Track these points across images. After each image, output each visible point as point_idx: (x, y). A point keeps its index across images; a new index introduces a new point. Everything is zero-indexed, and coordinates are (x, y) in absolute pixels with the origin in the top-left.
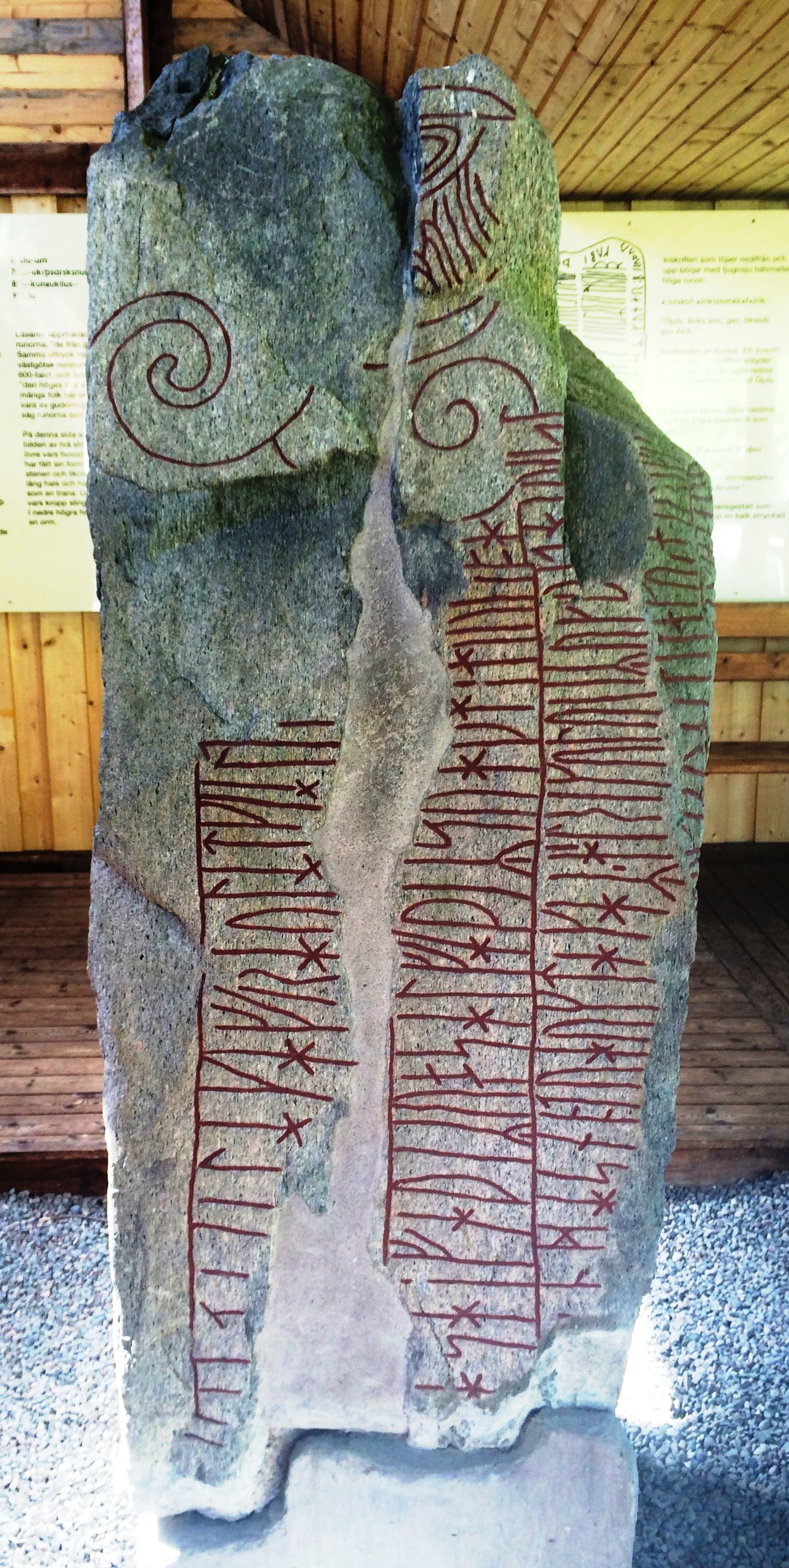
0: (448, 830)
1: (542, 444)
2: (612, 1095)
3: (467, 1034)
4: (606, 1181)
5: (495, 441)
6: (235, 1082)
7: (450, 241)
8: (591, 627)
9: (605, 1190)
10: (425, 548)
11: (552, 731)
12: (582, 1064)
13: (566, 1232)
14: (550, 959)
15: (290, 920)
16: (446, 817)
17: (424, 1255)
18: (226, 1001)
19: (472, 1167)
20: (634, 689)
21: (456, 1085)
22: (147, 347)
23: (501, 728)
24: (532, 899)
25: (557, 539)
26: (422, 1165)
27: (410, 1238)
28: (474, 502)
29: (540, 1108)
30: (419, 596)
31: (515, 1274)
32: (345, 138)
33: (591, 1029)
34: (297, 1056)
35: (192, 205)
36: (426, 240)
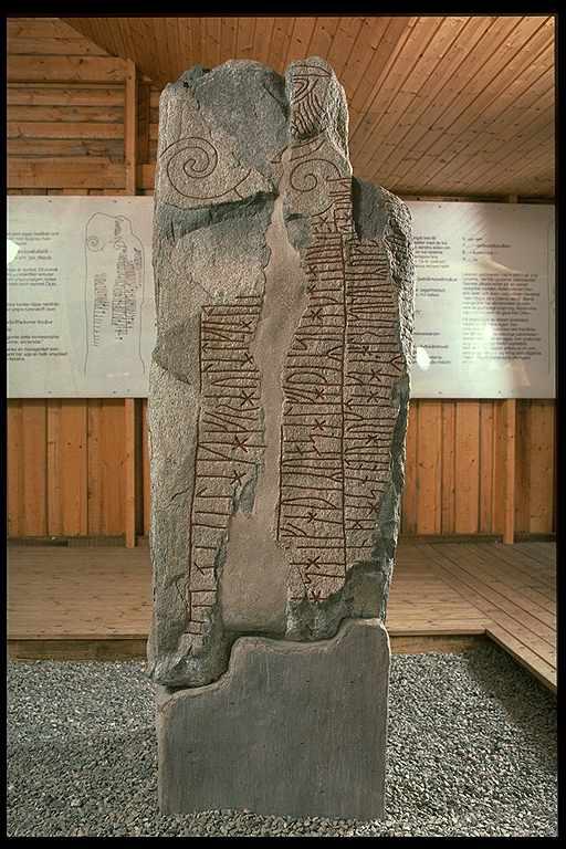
0: (307, 342)
1: (344, 189)
2: (376, 458)
3: (313, 432)
4: (374, 498)
5: (325, 189)
6: (213, 456)
7: (305, 118)
8: (364, 257)
9: (374, 502)
10: (294, 227)
11: (348, 299)
12: (364, 444)
13: (357, 521)
14: (350, 397)
15: (240, 382)
16: (305, 336)
17: (295, 535)
18: (209, 418)
19: (317, 493)
20: (383, 282)
21: (312, 455)
22: (185, 155)
23: (328, 298)
24: (342, 371)
25: (349, 222)
26: (295, 493)
27: (291, 528)
28: (315, 209)
29: (346, 464)
30: (294, 245)
31: (334, 542)
32: (264, 85)
33: (367, 428)
34: (238, 443)
35: (203, 107)
36: (296, 118)
